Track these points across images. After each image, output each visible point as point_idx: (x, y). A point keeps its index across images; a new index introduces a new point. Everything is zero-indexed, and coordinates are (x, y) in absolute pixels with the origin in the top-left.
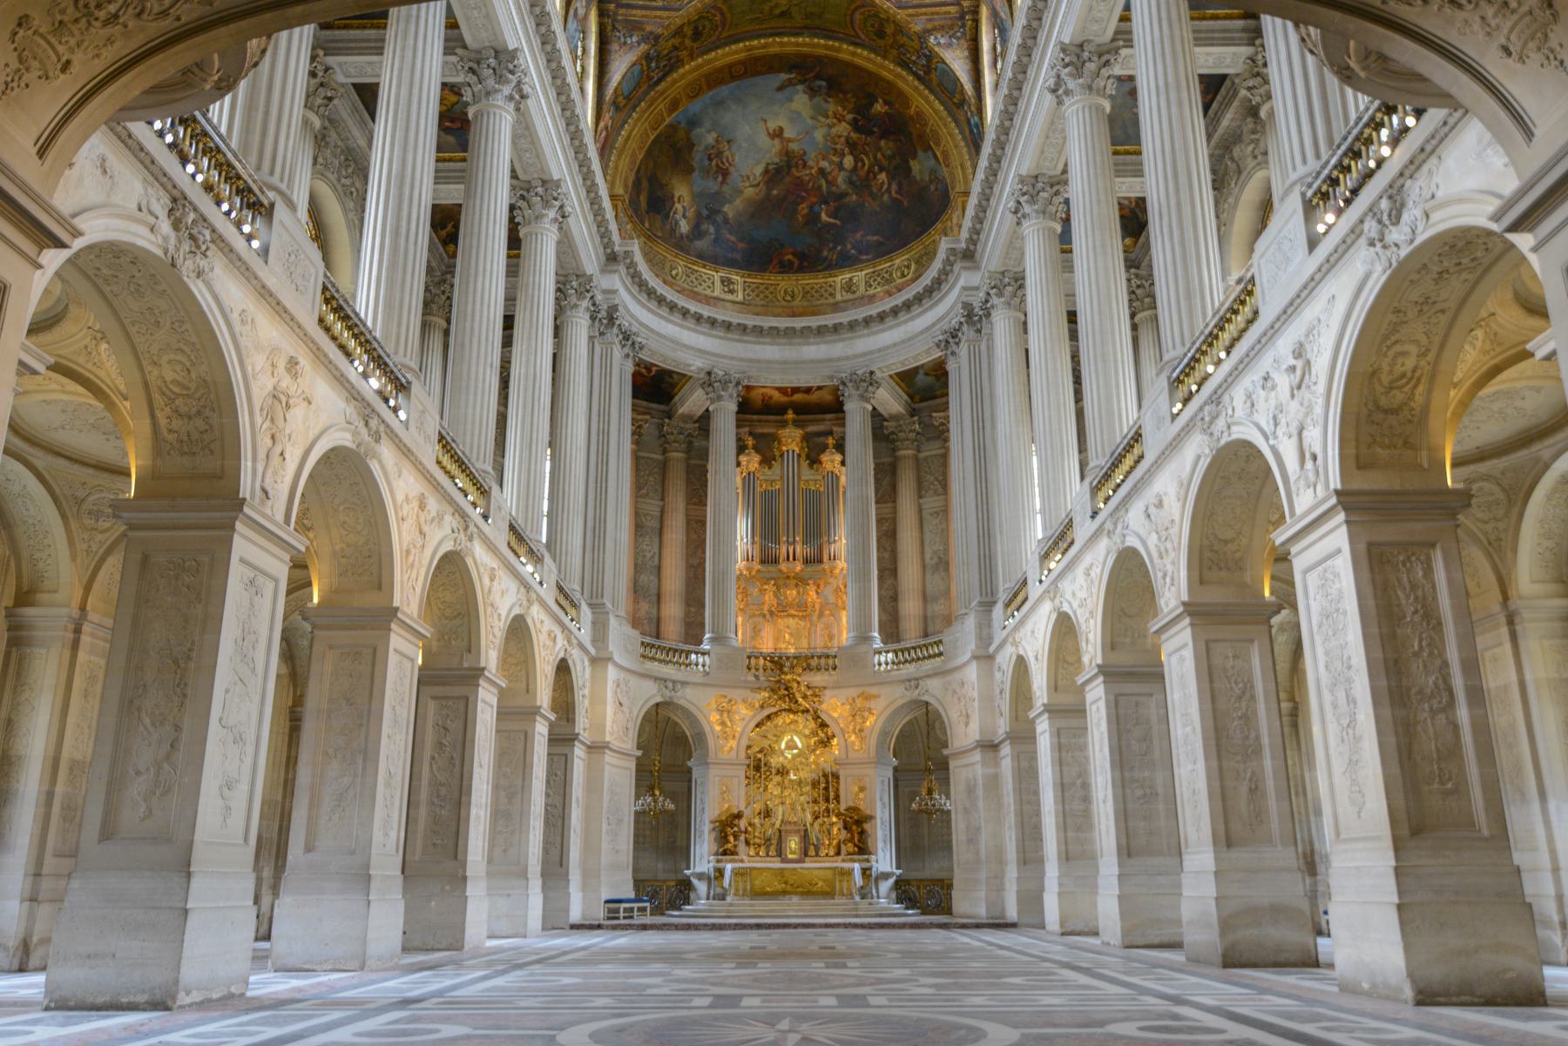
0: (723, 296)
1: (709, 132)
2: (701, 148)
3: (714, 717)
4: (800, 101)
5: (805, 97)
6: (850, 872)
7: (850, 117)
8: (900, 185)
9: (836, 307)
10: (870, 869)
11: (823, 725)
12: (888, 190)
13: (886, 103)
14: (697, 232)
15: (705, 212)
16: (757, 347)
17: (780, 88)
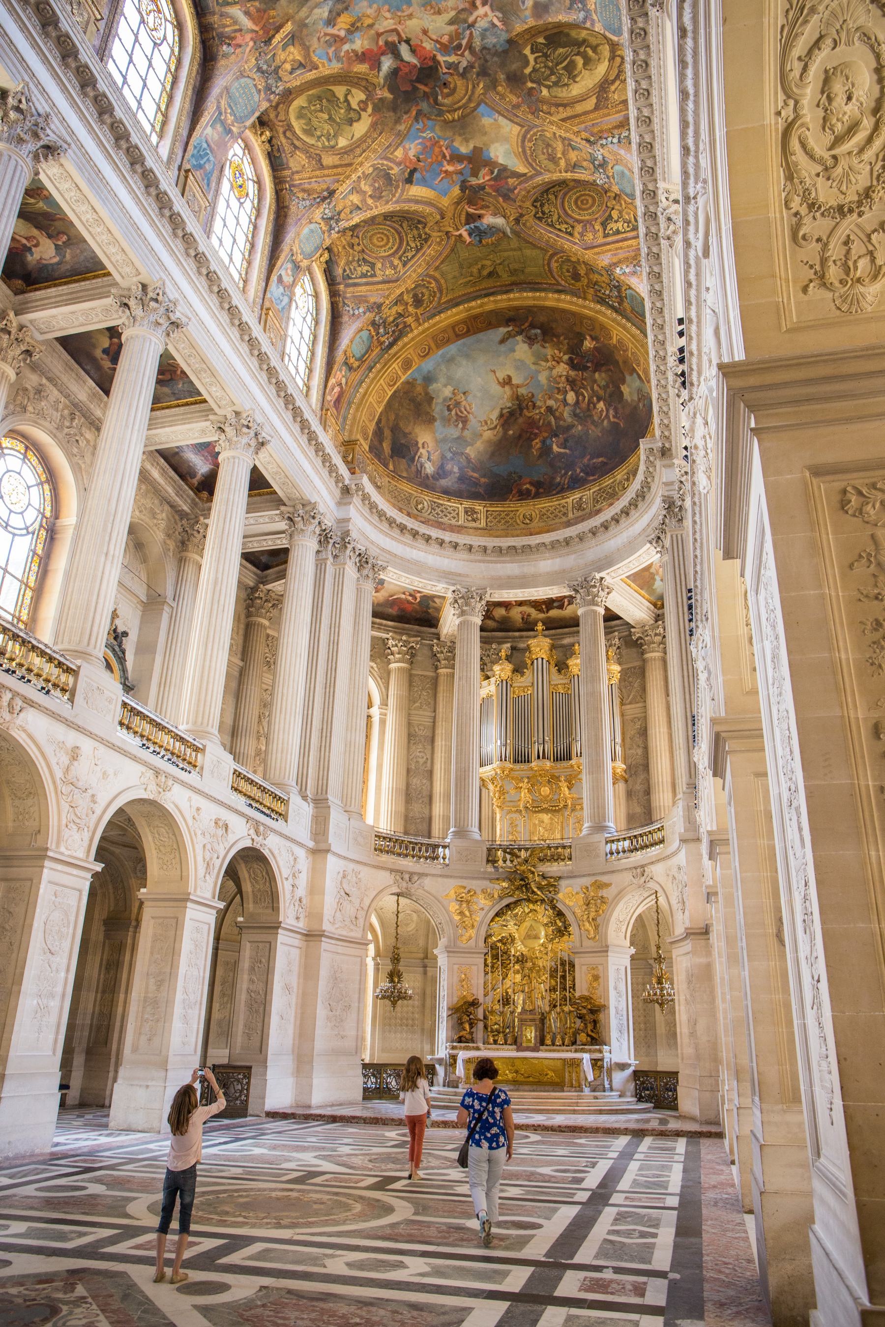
0: (466, 524)
1: (445, 386)
2: (440, 400)
3: (454, 907)
4: (522, 349)
5: (525, 347)
6: (576, 1064)
7: (566, 357)
8: (616, 410)
9: (569, 524)
10: (602, 1060)
11: (560, 914)
12: (607, 416)
13: (593, 338)
14: (441, 473)
15: (449, 455)
16: (499, 565)
17: (502, 341)
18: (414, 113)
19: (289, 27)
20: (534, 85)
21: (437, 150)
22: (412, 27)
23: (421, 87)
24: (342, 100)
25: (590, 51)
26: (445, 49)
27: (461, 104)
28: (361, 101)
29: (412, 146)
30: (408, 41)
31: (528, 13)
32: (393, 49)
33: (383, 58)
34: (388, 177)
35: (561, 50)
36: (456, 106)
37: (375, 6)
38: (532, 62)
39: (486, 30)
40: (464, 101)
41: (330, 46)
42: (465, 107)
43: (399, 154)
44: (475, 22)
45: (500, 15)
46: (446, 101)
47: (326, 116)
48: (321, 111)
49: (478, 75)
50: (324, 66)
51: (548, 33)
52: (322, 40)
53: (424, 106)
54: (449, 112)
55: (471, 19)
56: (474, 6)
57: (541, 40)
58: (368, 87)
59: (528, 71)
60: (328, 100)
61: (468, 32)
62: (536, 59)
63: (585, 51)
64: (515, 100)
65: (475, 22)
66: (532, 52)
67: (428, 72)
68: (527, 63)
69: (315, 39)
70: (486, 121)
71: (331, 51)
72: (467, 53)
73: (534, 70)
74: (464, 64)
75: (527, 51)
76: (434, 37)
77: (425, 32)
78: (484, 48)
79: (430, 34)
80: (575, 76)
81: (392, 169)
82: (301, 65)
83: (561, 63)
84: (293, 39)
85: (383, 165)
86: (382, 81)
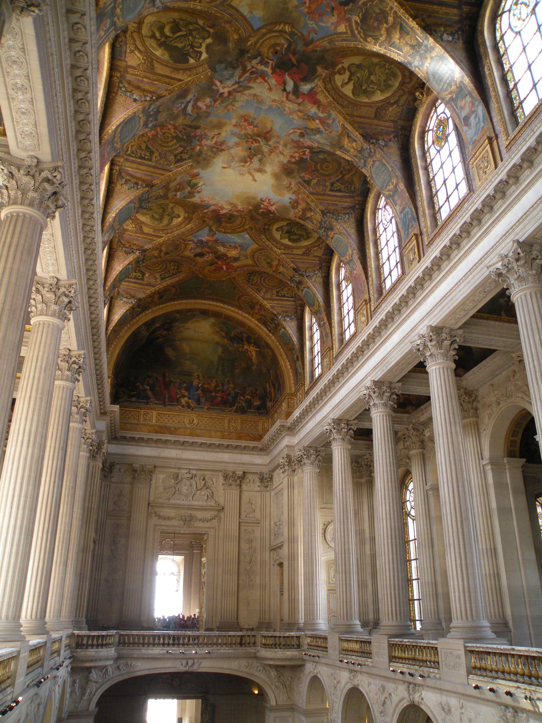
18: (310, 47)
19: (338, 153)
20: (208, 29)
21: (313, 7)
22: (277, 95)
23: (294, 60)
24: (353, 82)
25: (158, 35)
26: (263, 75)
27: (273, 34)
28: (340, 74)
29: (329, 25)
30: (284, 90)
31: (194, 90)
32: (296, 91)
33: (306, 92)
34: (364, 20)
35: (180, 45)
36: (277, 34)
37: (291, 117)
38: (204, 46)
39: (228, 79)
40: (269, 36)
41: (328, 124)
42: (270, 31)
43: (342, 28)
44: (233, 85)
45: (214, 87)
46: (283, 41)
47: (372, 77)
48: (372, 82)
49: (248, 51)
50: (339, 122)
51: (185, 66)
52: (329, 130)
53: (300, 47)
54: (285, 32)
55: (236, 86)
56: (230, 93)
57: (192, 61)
58: (329, 81)
59: (209, 41)
60: (361, 87)
61: (241, 80)
62: (200, 47)
63: (161, 37)
64: (227, 26)
65: (233, 85)
66: (201, 53)
67: (283, 66)
68: (208, 47)
69: (332, 134)
70: (259, 13)
71: (330, 122)
72: (249, 67)
73: (204, 39)
74: (254, 62)
75: (204, 56)
76: (266, 84)
77: (270, 89)
78: (234, 68)
79: (268, 87)
80: (173, 22)
81: (356, 22)
82: (349, 137)
83: (182, 36)
84: (341, 148)
85: (359, 33)
86: (316, 81)
